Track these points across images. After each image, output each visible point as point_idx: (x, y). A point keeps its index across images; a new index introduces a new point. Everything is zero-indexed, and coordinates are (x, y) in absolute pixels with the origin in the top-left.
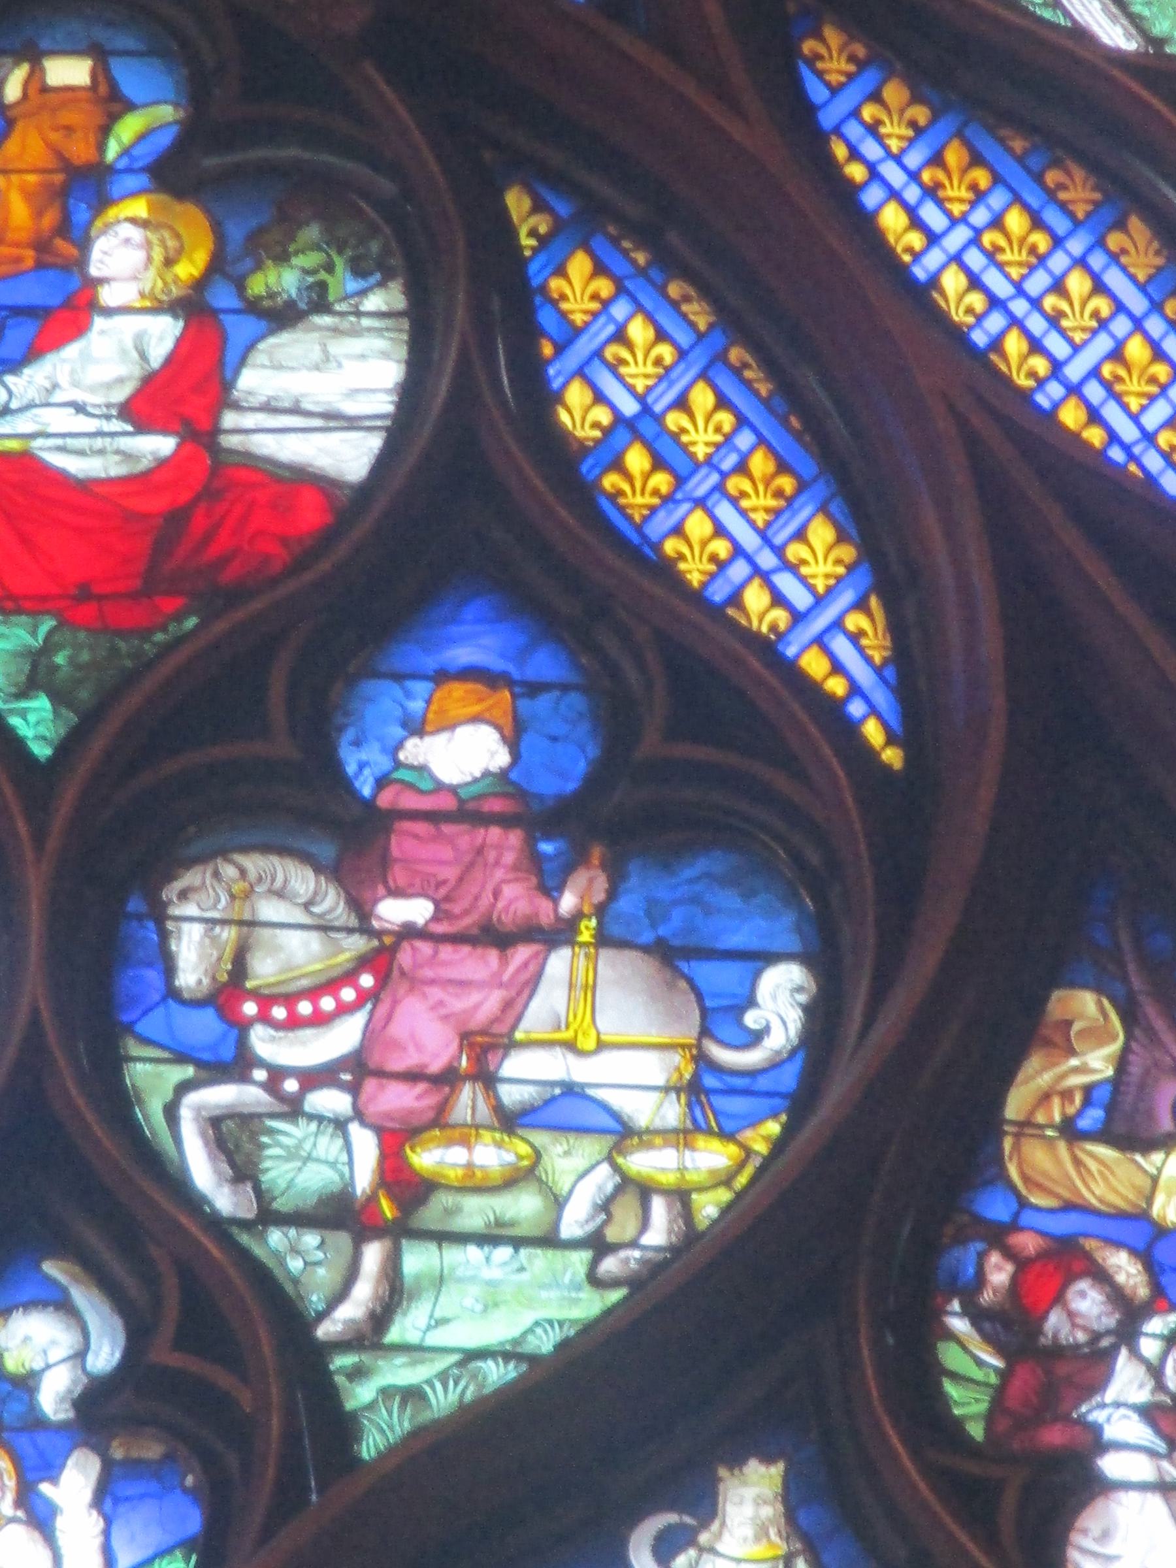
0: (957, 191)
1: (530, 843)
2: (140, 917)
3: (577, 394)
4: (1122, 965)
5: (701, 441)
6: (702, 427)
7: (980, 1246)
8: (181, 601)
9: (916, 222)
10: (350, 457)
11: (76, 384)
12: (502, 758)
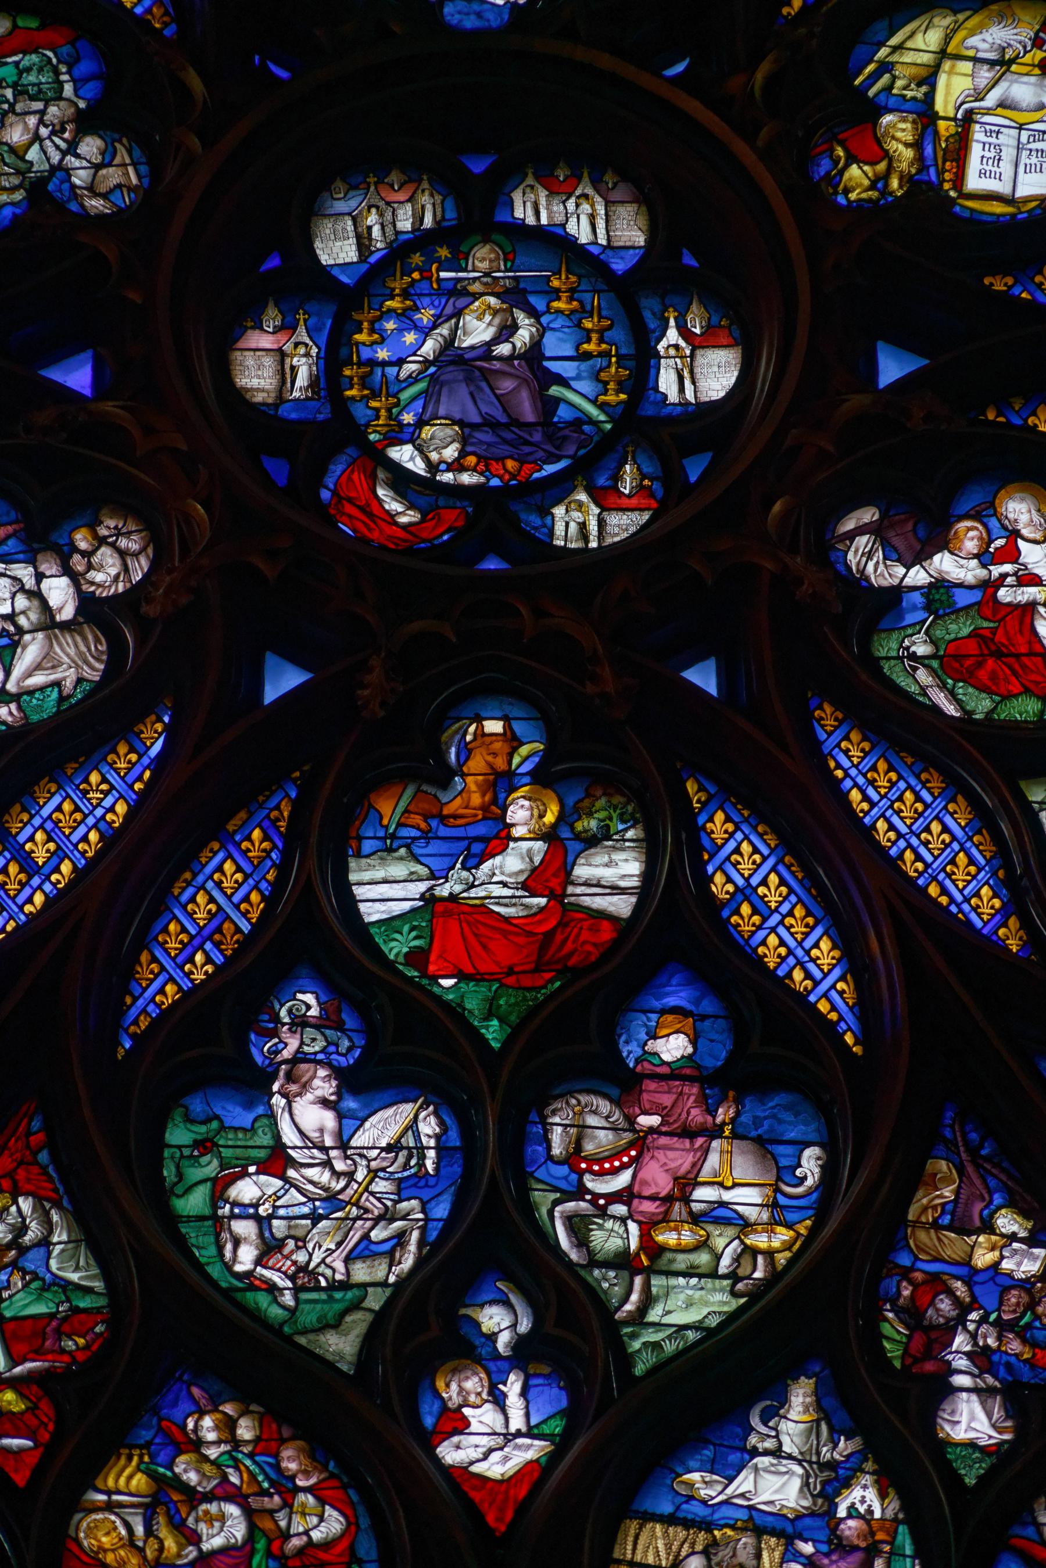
0: (883, 782)
1: (702, 1089)
2: (535, 1123)
3: (719, 878)
4: (958, 1147)
5: (773, 900)
6: (772, 894)
7: (898, 1278)
8: (548, 976)
9: (866, 798)
10: (622, 906)
11: (503, 873)
12: (690, 1050)
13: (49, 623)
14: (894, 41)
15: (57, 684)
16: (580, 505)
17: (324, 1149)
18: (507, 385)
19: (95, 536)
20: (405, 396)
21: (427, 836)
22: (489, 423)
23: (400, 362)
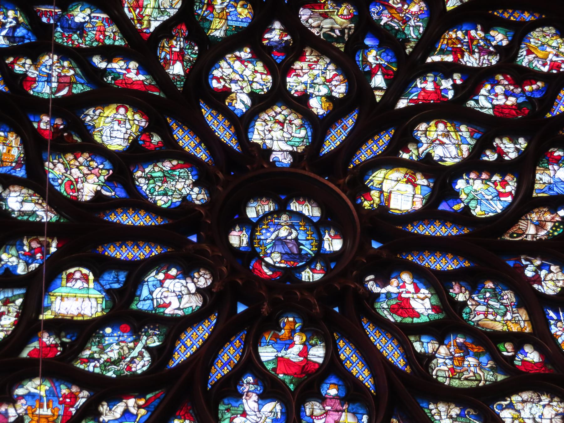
3: (342, 355)
5: (354, 360)
6: (354, 359)
8: (304, 375)
9: (374, 339)
10: (320, 361)
12: (337, 392)
13: (189, 293)
14: (373, 175)
15: (192, 307)
16: (308, 272)
17: (255, 412)
18: (290, 245)
19: (199, 274)
20: (268, 247)
21: (276, 343)
22: (287, 253)
23: (266, 239)
